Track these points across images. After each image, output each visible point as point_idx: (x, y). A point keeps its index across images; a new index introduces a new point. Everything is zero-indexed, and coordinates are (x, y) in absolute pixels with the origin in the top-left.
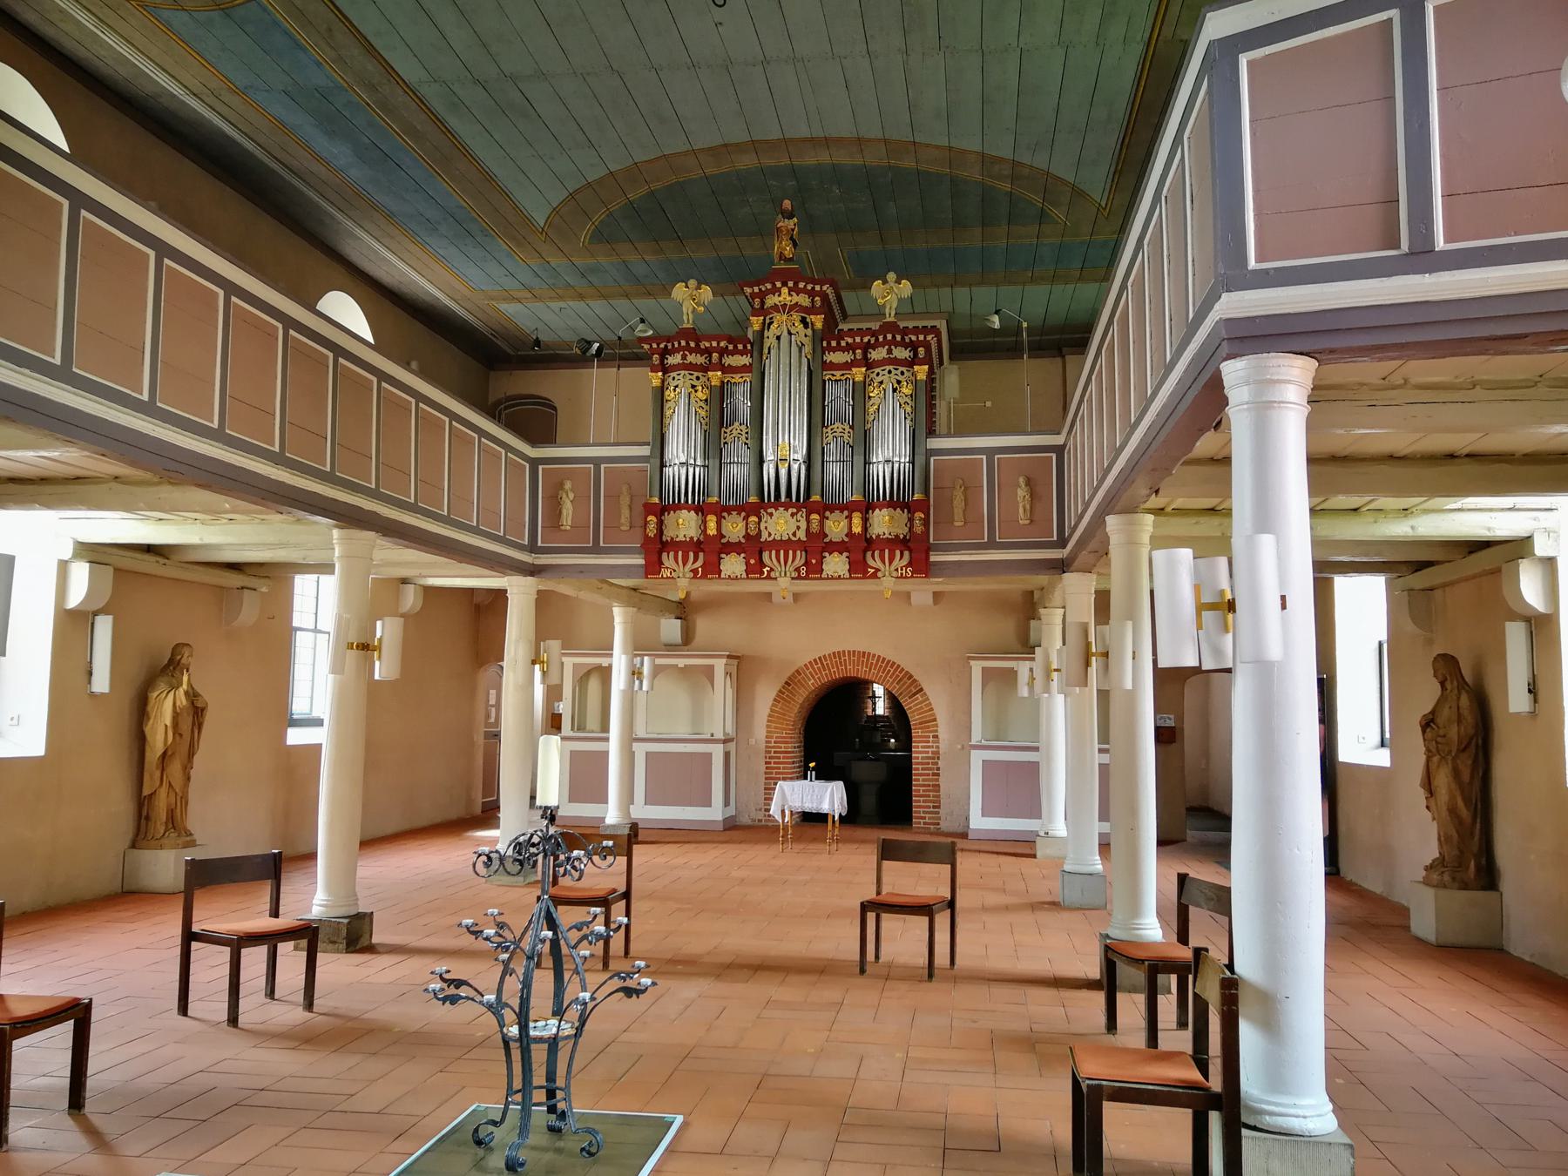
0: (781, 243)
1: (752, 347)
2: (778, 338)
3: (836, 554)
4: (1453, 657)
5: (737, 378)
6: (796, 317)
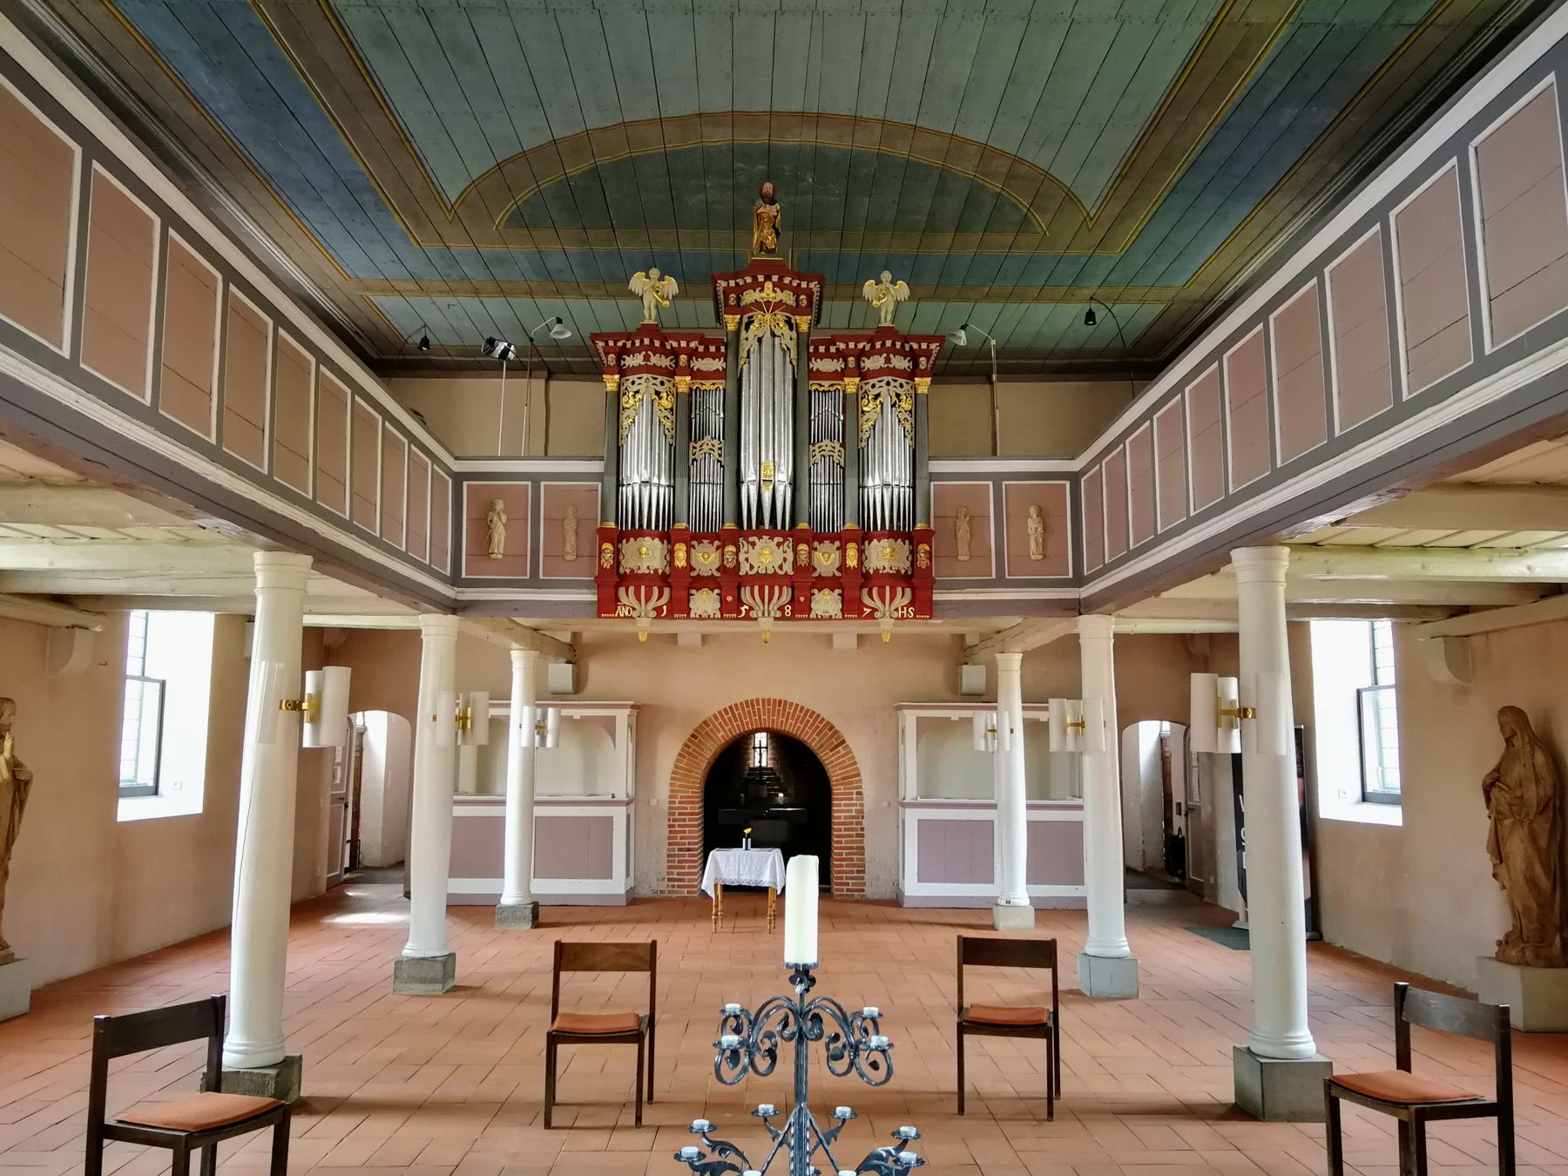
0: (762, 231)
1: (726, 349)
2: (760, 340)
3: (826, 591)
4: (1522, 711)
5: (708, 385)
6: (781, 316)
